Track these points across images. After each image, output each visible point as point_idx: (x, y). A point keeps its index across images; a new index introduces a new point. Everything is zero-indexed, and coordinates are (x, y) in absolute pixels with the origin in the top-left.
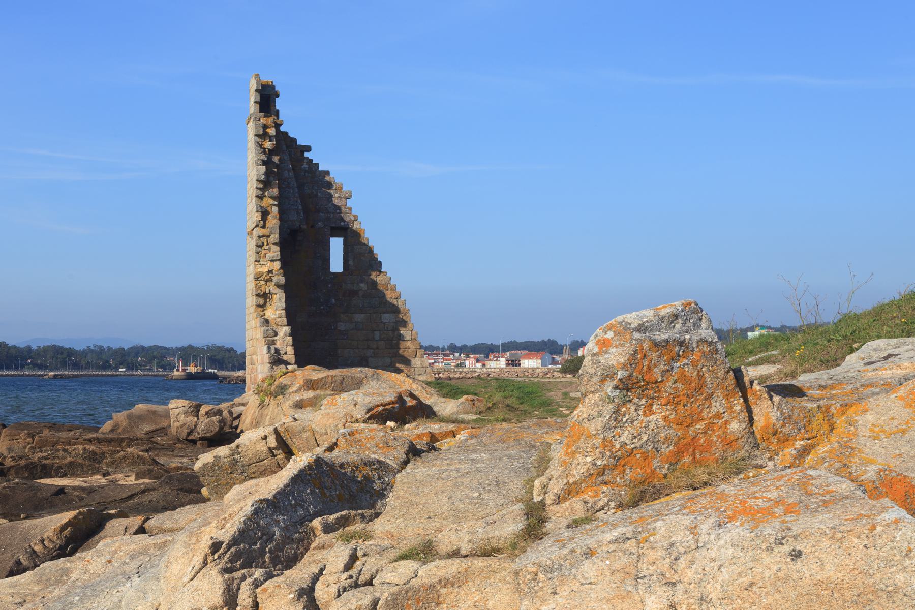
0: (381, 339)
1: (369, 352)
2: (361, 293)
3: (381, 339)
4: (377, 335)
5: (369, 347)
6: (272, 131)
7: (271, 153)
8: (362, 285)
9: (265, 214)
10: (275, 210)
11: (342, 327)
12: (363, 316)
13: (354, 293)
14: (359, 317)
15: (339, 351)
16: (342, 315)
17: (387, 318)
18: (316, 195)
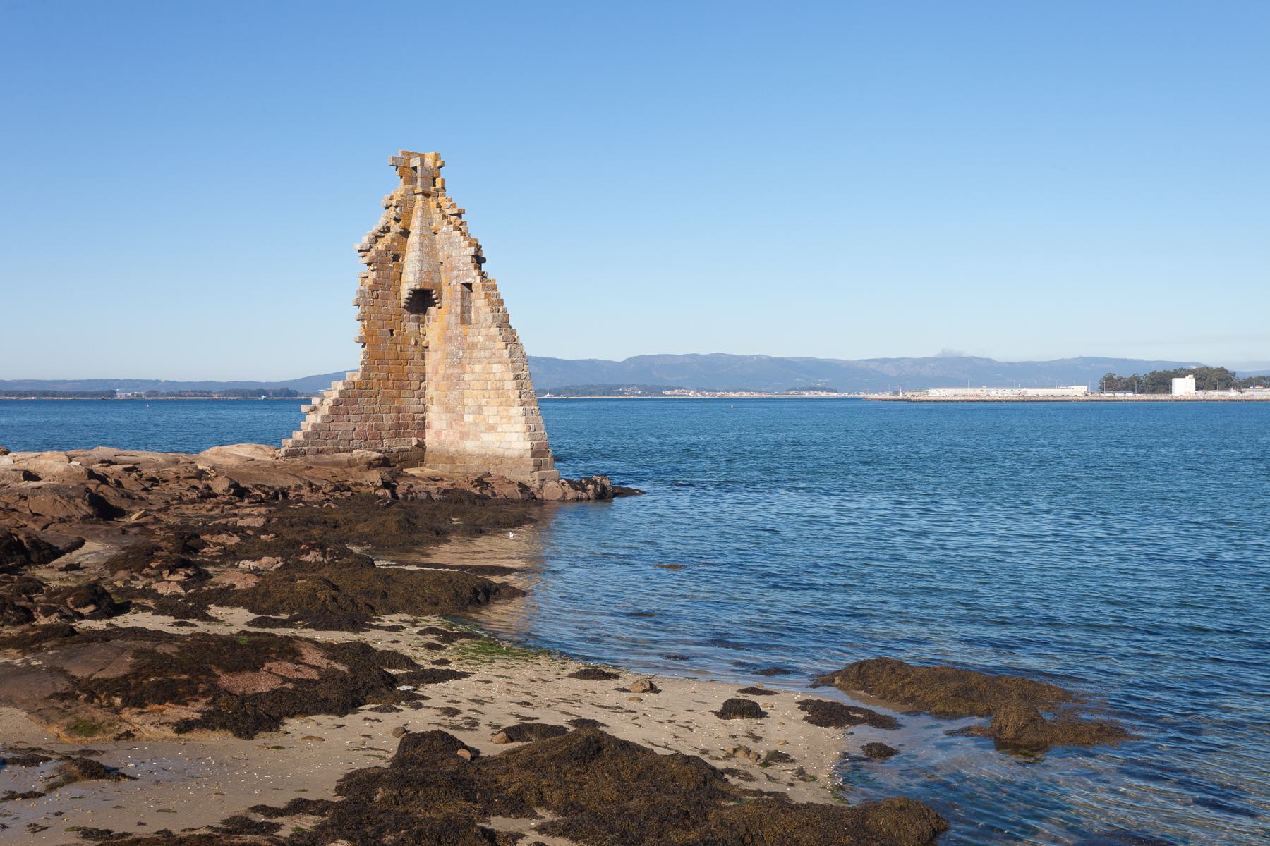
1: (483, 402)
14: (478, 368)
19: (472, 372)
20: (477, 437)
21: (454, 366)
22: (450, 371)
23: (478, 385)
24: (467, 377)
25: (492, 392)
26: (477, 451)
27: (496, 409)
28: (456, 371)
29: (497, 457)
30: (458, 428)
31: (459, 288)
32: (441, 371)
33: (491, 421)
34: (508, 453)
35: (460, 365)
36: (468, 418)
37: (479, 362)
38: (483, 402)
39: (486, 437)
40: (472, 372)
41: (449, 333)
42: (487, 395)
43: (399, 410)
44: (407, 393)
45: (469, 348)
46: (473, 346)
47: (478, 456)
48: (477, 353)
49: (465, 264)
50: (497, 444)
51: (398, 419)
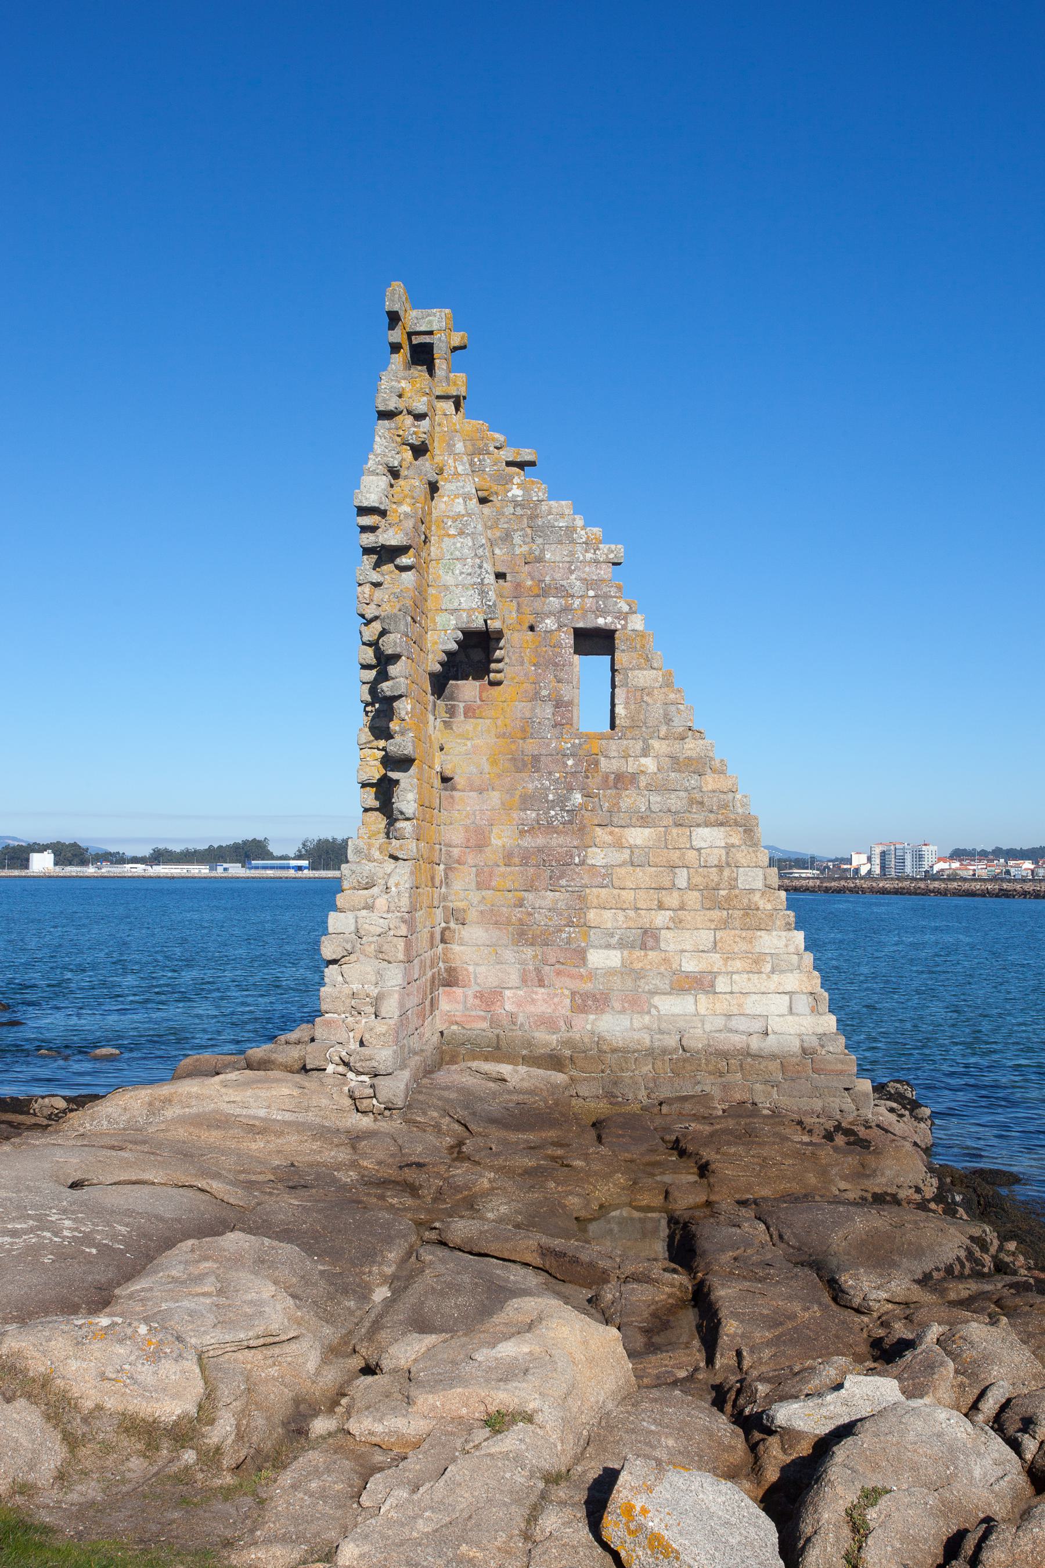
1: (661, 918)
2: (643, 781)
3: (691, 887)
4: (682, 878)
5: (661, 907)
14: (638, 836)
15: (592, 915)
18: (540, 560)
19: (619, 845)
20: (635, 1003)
21: (550, 828)
22: (528, 842)
23: (643, 876)
24: (597, 857)
27: (706, 937)
28: (556, 840)
29: (724, 1055)
30: (564, 986)
32: (502, 838)
33: (690, 966)
34: (771, 1043)
35: (576, 824)
37: (644, 820)
38: (661, 918)
41: (531, 747)
45: (605, 784)
46: (621, 781)
47: (651, 1053)
48: (630, 799)
50: (720, 1022)
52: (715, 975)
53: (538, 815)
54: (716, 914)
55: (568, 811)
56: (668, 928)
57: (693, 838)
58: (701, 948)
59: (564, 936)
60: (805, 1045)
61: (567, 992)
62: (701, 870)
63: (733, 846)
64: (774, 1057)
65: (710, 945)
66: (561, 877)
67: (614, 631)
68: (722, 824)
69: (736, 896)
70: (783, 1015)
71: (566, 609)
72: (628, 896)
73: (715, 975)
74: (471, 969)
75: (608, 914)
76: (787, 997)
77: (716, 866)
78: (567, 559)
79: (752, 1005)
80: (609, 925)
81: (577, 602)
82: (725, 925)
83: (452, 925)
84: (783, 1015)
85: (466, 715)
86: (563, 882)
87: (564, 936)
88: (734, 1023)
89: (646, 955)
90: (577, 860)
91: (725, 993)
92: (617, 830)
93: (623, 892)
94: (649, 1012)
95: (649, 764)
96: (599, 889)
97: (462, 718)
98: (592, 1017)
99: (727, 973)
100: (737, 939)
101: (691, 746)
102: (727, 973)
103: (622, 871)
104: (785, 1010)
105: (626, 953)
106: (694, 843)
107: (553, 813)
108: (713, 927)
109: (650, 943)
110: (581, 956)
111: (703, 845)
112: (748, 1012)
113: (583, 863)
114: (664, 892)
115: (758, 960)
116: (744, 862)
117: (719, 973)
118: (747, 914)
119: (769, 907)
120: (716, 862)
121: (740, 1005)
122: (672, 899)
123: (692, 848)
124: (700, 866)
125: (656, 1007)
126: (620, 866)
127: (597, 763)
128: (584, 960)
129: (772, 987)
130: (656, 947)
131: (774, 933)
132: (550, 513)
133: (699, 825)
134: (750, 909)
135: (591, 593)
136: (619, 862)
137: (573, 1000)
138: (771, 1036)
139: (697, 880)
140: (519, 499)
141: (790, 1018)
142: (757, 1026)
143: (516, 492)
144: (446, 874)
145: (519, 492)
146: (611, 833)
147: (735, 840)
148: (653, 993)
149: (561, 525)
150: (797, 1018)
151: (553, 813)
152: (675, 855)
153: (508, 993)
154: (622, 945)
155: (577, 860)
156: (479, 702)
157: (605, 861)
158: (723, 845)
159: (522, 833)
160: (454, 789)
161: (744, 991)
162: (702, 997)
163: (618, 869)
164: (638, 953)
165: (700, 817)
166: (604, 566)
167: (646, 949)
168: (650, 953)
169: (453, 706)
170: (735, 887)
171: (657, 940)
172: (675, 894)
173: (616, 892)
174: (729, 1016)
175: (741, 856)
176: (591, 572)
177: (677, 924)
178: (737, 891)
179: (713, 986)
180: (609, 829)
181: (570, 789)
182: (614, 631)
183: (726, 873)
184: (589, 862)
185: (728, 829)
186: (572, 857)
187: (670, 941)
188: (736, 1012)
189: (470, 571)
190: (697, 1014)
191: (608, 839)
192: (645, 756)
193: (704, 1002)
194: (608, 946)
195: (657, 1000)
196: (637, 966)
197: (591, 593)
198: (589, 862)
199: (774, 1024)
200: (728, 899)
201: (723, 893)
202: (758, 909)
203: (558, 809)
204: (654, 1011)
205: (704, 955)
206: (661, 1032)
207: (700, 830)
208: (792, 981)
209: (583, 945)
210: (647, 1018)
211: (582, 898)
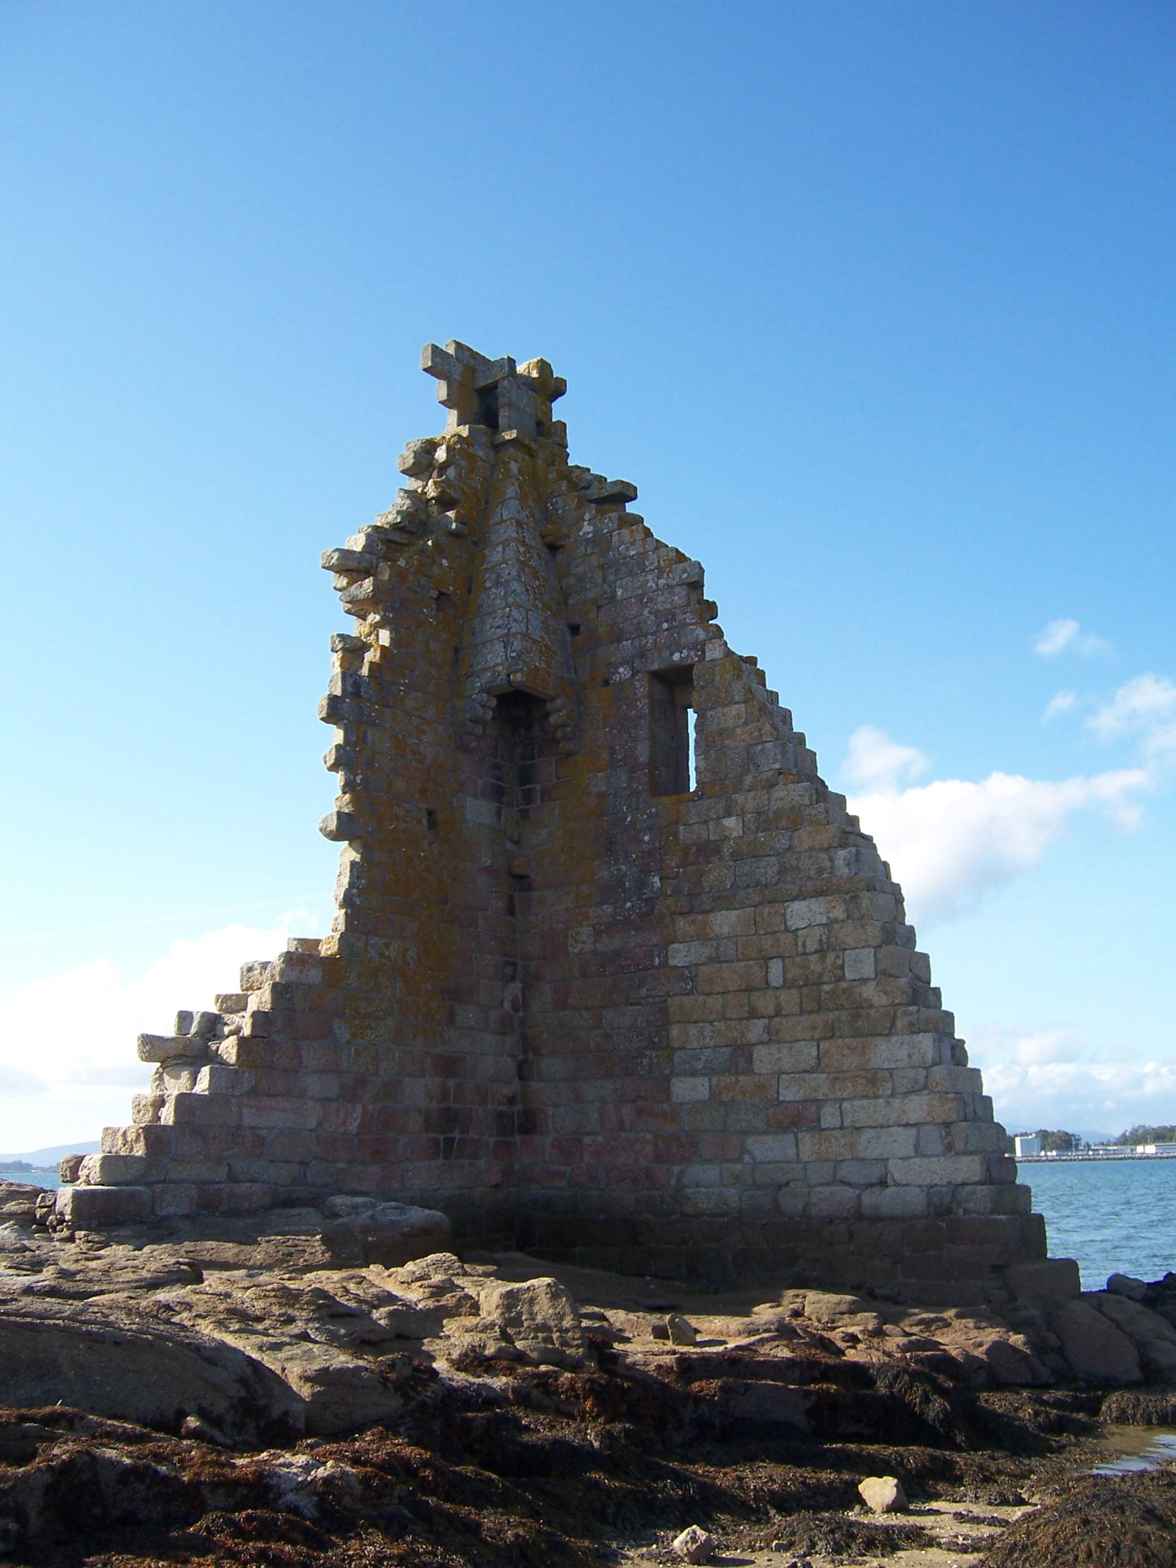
0: (788, 984)
1: (756, 1029)
2: (726, 850)
4: (776, 972)
5: (753, 1014)
6: (441, 455)
7: (445, 502)
8: (731, 822)
9: (352, 649)
10: (385, 637)
11: (680, 955)
12: (733, 915)
13: (709, 850)
14: (725, 921)
15: (675, 1031)
16: (681, 923)
17: (805, 914)
19: (703, 936)
24: (680, 955)
25: (790, 999)
26: (733, 1196)
31: (642, 687)
33: (790, 1093)
36: (689, 1089)
39: (769, 1149)
40: (703, 936)
42: (765, 1003)
43: (448, 1066)
44: (467, 1014)
49: (670, 615)
51: (444, 1095)
52: (819, 1103)
53: (615, 908)
54: (819, 1019)
55: (646, 900)
56: (761, 1043)
57: (788, 916)
58: (802, 1066)
59: (646, 1061)
60: (935, 1200)
61: (649, 1136)
62: (798, 959)
63: (836, 921)
64: (894, 1219)
65: (813, 1062)
66: (640, 987)
67: (692, 666)
68: (819, 893)
69: (844, 990)
70: (908, 1158)
71: (642, 654)
72: (715, 1003)
73: (819, 1103)
74: (550, 1111)
75: (693, 1030)
76: (914, 1131)
77: (816, 952)
78: (640, 592)
79: (869, 1145)
80: (695, 1045)
81: (651, 639)
82: (831, 1033)
83: (531, 1057)
84: (908, 1158)
85: (543, 800)
86: (643, 992)
87: (646, 1061)
88: (843, 1173)
89: (737, 1081)
90: (657, 961)
91: (834, 1129)
92: (700, 917)
93: (710, 1000)
94: (739, 1160)
95: (731, 823)
96: (684, 998)
97: (539, 803)
98: (676, 1169)
99: (836, 1100)
100: (846, 1051)
101: (782, 794)
102: (836, 1100)
103: (705, 971)
104: (909, 1150)
105: (715, 1080)
106: (789, 923)
107: (629, 905)
108: (816, 1036)
109: (742, 1064)
110: (664, 1086)
111: (801, 924)
112: (862, 1155)
113: (664, 964)
114: (756, 994)
115: (873, 1078)
116: (850, 941)
117: (825, 1101)
118: (857, 1016)
119: (885, 1000)
120: (816, 946)
121: (852, 1146)
122: (765, 1003)
123: (787, 930)
124: (798, 955)
125: (750, 1153)
126: (705, 964)
127: (676, 837)
128: (668, 1092)
129: (893, 1118)
130: (749, 1071)
131: (894, 1039)
132: (621, 543)
133: (795, 899)
134: (860, 1007)
135: (665, 626)
136: (704, 959)
137: (656, 1145)
138: (890, 1190)
139: (794, 972)
140: (590, 536)
141: (917, 1160)
142: (875, 1173)
143: (587, 528)
144: (523, 994)
145: (591, 529)
146: (693, 922)
147: (838, 913)
148: (745, 1133)
149: (632, 553)
150: (926, 1161)
151: (629, 905)
152: (767, 943)
153: (587, 1140)
154: (709, 1071)
155: (657, 961)
156: (555, 780)
157: (687, 959)
158: (824, 921)
159: (598, 934)
160: (529, 889)
161: (858, 1125)
162: (806, 1139)
163: (706, 968)
164: (728, 1079)
165: (795, 890)
166: (678, 589)
167: (737, 1073)
168: (741, 1078)
169: (529, 790)
170: (842, 978)
171: (750, 1060)
172: (770, 993)
173: (701, 998)
174: (838, 1163)
175: (847, 933)
176: (663, 602)
177: (772, 1037)
178: (844, 985)
179: (819, 1120)
180: (691, 918)
181: (646, 871)
182: (692, 666)
183: (830, 959)
184: (671, 963)
185: (829, 898)
186: (652, 960)
187: (764, 1059)
188: (848, 1156)
189: (500, 622)
190: (798, 1160)
191: (691, 930)
192: (730, 816)
193: (808, 1145)
194: (694, 1073)
195: (753, 1143)
196: (726, 1098)
197: (665, 626)
198: (671, 963)
199: (897, 1171)
200: (833, 994)
201: (826, 987)
202: (871, 1006)
203: (635, 898)
204: (747, 1158)
205: (806, 1076)
206: (756, 1185)
207: (796, 906)
208: (917, 1107)
209: (667, 1072)
210: (738, 1167)
211: (664, 1012)
